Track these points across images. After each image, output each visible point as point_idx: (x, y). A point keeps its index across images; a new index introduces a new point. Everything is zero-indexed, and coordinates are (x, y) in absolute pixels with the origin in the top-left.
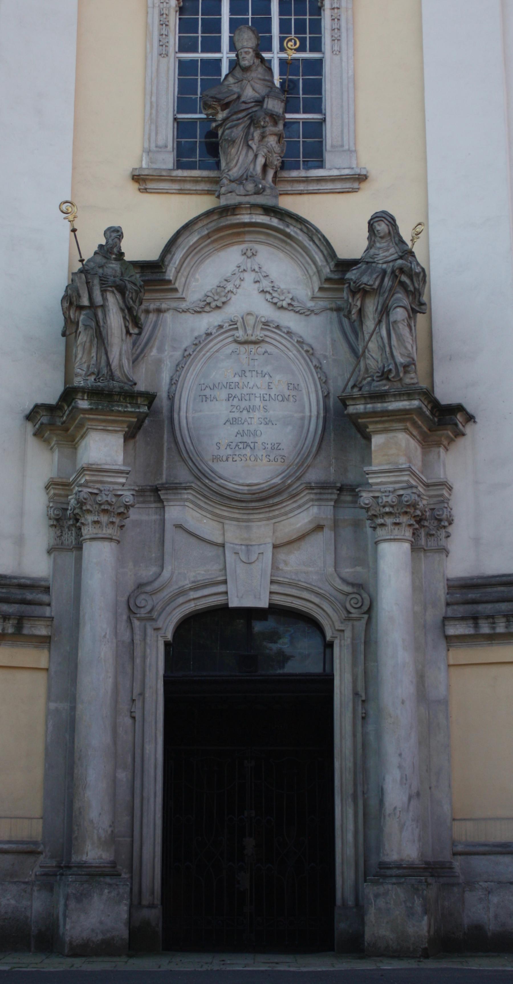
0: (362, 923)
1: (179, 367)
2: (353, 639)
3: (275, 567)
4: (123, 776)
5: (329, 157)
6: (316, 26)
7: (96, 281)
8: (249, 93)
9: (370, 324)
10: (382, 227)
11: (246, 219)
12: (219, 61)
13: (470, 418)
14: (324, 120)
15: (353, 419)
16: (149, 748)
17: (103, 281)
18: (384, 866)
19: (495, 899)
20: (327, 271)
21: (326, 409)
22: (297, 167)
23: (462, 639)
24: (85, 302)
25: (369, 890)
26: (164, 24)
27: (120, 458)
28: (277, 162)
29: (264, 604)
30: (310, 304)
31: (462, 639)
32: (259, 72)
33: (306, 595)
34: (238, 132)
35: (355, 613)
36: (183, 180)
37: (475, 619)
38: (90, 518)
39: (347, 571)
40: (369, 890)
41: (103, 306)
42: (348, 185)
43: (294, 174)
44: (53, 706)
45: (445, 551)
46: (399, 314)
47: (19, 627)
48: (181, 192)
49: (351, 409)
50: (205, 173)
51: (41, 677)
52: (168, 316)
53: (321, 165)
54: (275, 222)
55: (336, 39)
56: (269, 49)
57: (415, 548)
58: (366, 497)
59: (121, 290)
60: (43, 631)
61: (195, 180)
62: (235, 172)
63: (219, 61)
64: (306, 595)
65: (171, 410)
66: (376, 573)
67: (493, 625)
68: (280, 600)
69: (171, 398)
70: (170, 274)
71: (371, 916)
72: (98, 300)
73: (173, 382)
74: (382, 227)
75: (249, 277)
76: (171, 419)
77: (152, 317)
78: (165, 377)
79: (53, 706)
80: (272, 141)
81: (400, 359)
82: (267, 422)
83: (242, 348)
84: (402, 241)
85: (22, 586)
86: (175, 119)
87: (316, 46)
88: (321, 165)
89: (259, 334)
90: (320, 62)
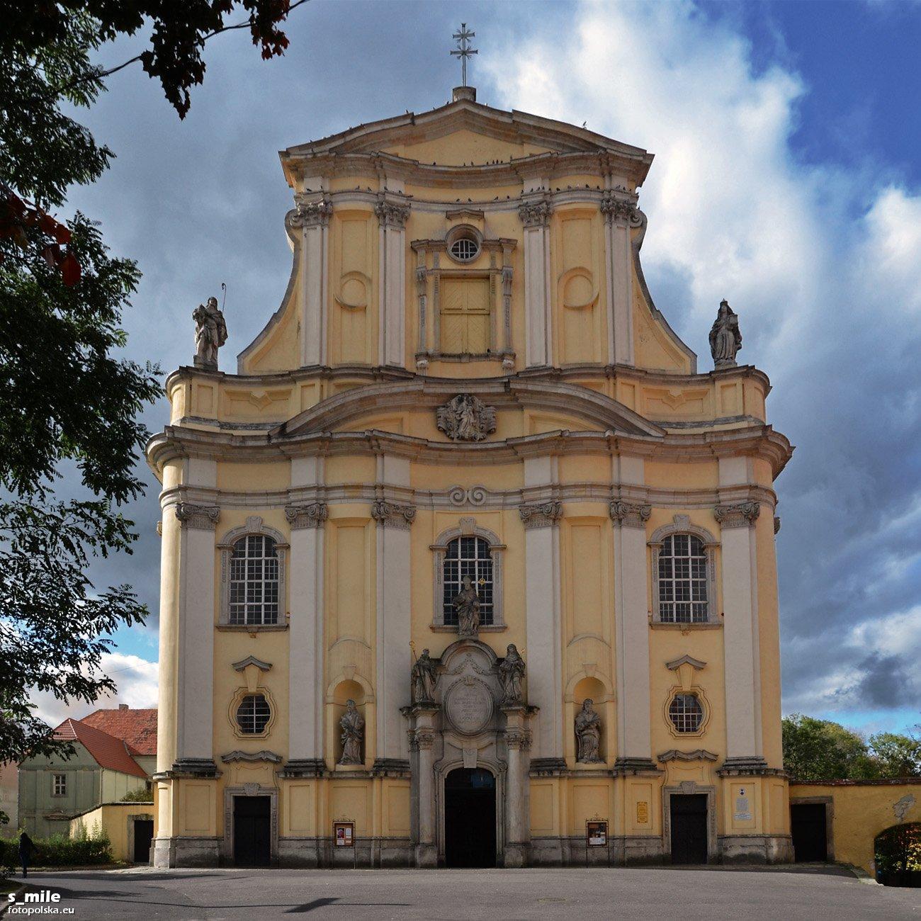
0: (504, 858)
1: (447, 693)
2: (502, 777)
3: (478, 756)
4: (434, 818)
5: (495, 621)
6: (490, 571)
7: (421, 668)
8: (469, 599)
9: (508, 681)
10: (511, 650)
11: (468, 644)
12: (458, 584)
13: (539, 709)
14: (493, 606)
15: (503, 712)
16: (441, 810)
17: (424, 667)
18: (510, 843)
19: (542, 852)
20: (494, 661)
21: (494, 706)
22: (484, 624)
23: (535, 778)
24: (419, 675)
25: (506, 849)
26: (439, 572)
27: (431, 724)
28: (478, 623)
29: (475, 767)
30: (489, 672)
31: (535, 778)
32: (472, 591)
33: (487, 764)
34: (465, 614)
35: (502, 770)
36: (447, 628)
37: (538, 771)
38: (422, 743)
39: (500, 757)
40: (506, 849)
41: (424, 676)
42: (501, 630)
43: (483, 626)
44: (412, 798)
45: (528, 751)
46: (516, 679)
47: (401, 775)
48: (446, 632)
49: (501, 709)
50: (454, 626)
51: (408, 789)
52: (443, 677)
53: (491, 623)
54: (478, 645)
55: (497, 578)
56: (475, 580)
57: (521, 750)
58: (506, 736)
59: (430, 670)
60: (409, 776)
61: (451, 628)
62: (464, 627)
63: (458, 584)
64: (487, 764)
65: (445, 707)
66: (508, 757)
67: (543, 774)
68: (479, 766)
69: (445, 703)
70: (444, 663)
71: (507, 857)
72: (422, 674)
73: (445, 698)
74: (511, 650)
75: (469, 663)
76: (445, 711)
77: (438, 676)
78: (443, 696)
79: (412, 798)
80: (476, 616)
81: (517, 693)
82: (476, 711)
83: (467, 687)
84: (517, 654)
85: (401, 762)
86: (444, 606)
87: (490, 579)
88: (491, 623)
89: (473, 682)
90: (492, 584)
